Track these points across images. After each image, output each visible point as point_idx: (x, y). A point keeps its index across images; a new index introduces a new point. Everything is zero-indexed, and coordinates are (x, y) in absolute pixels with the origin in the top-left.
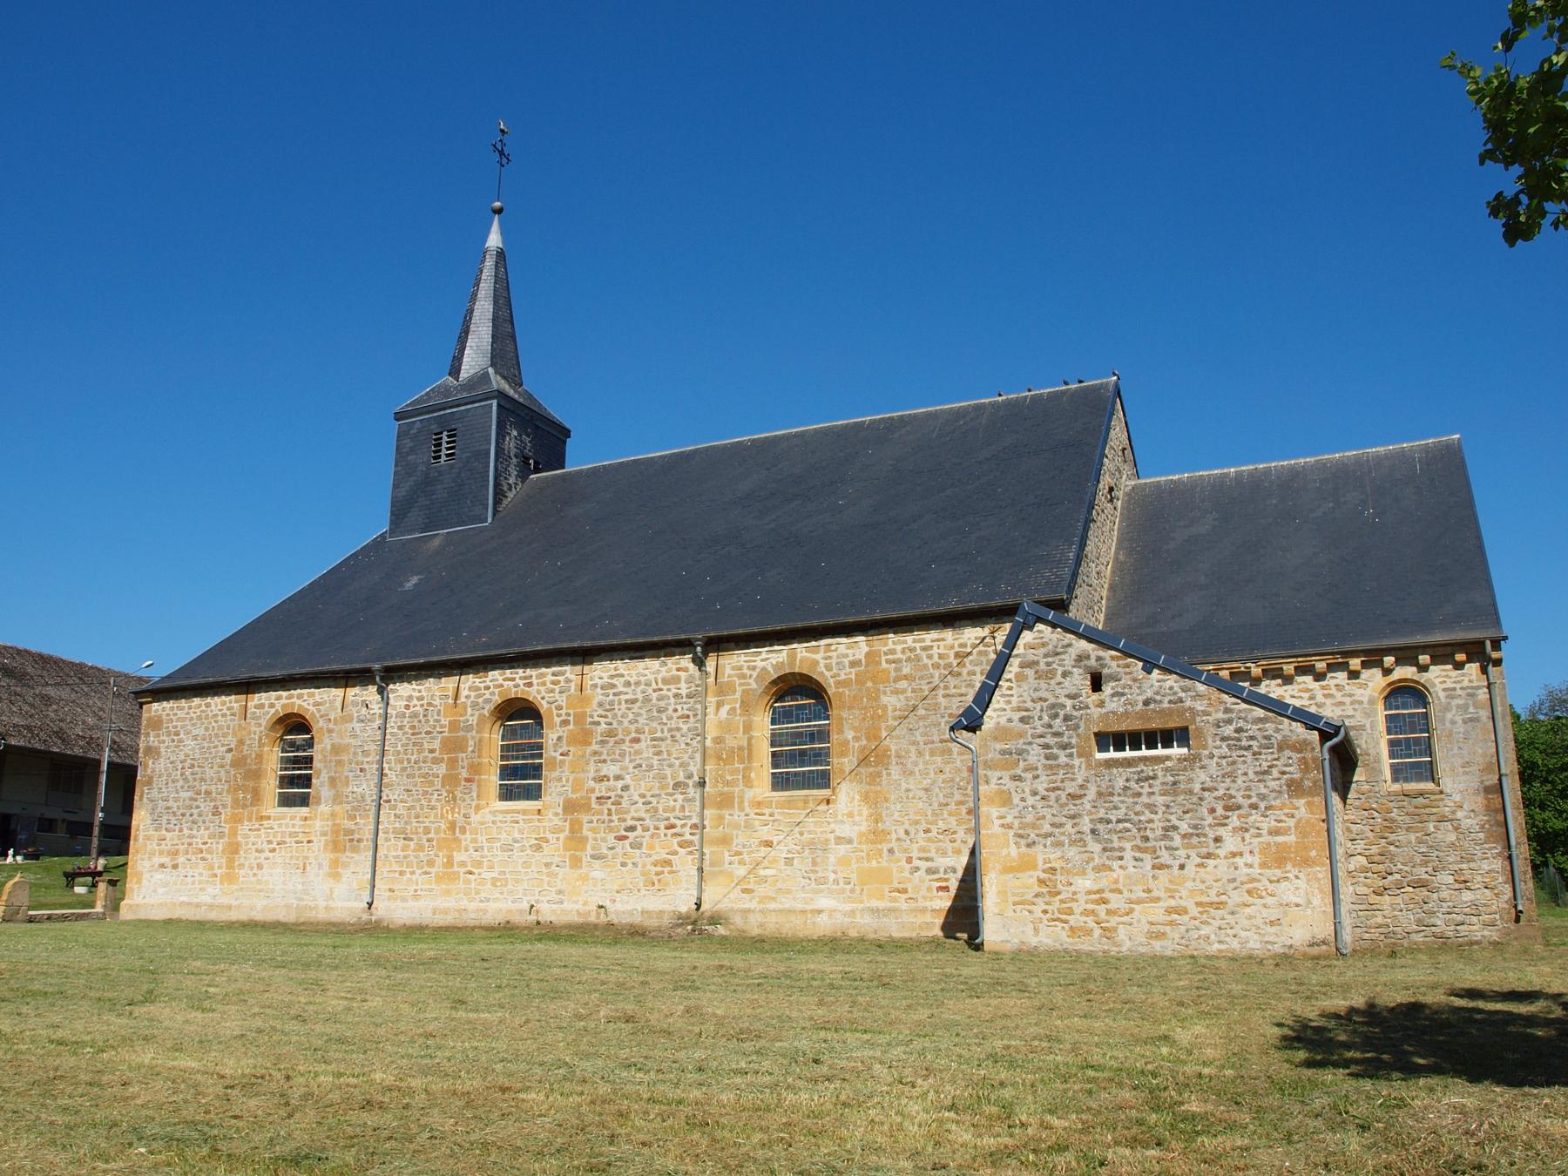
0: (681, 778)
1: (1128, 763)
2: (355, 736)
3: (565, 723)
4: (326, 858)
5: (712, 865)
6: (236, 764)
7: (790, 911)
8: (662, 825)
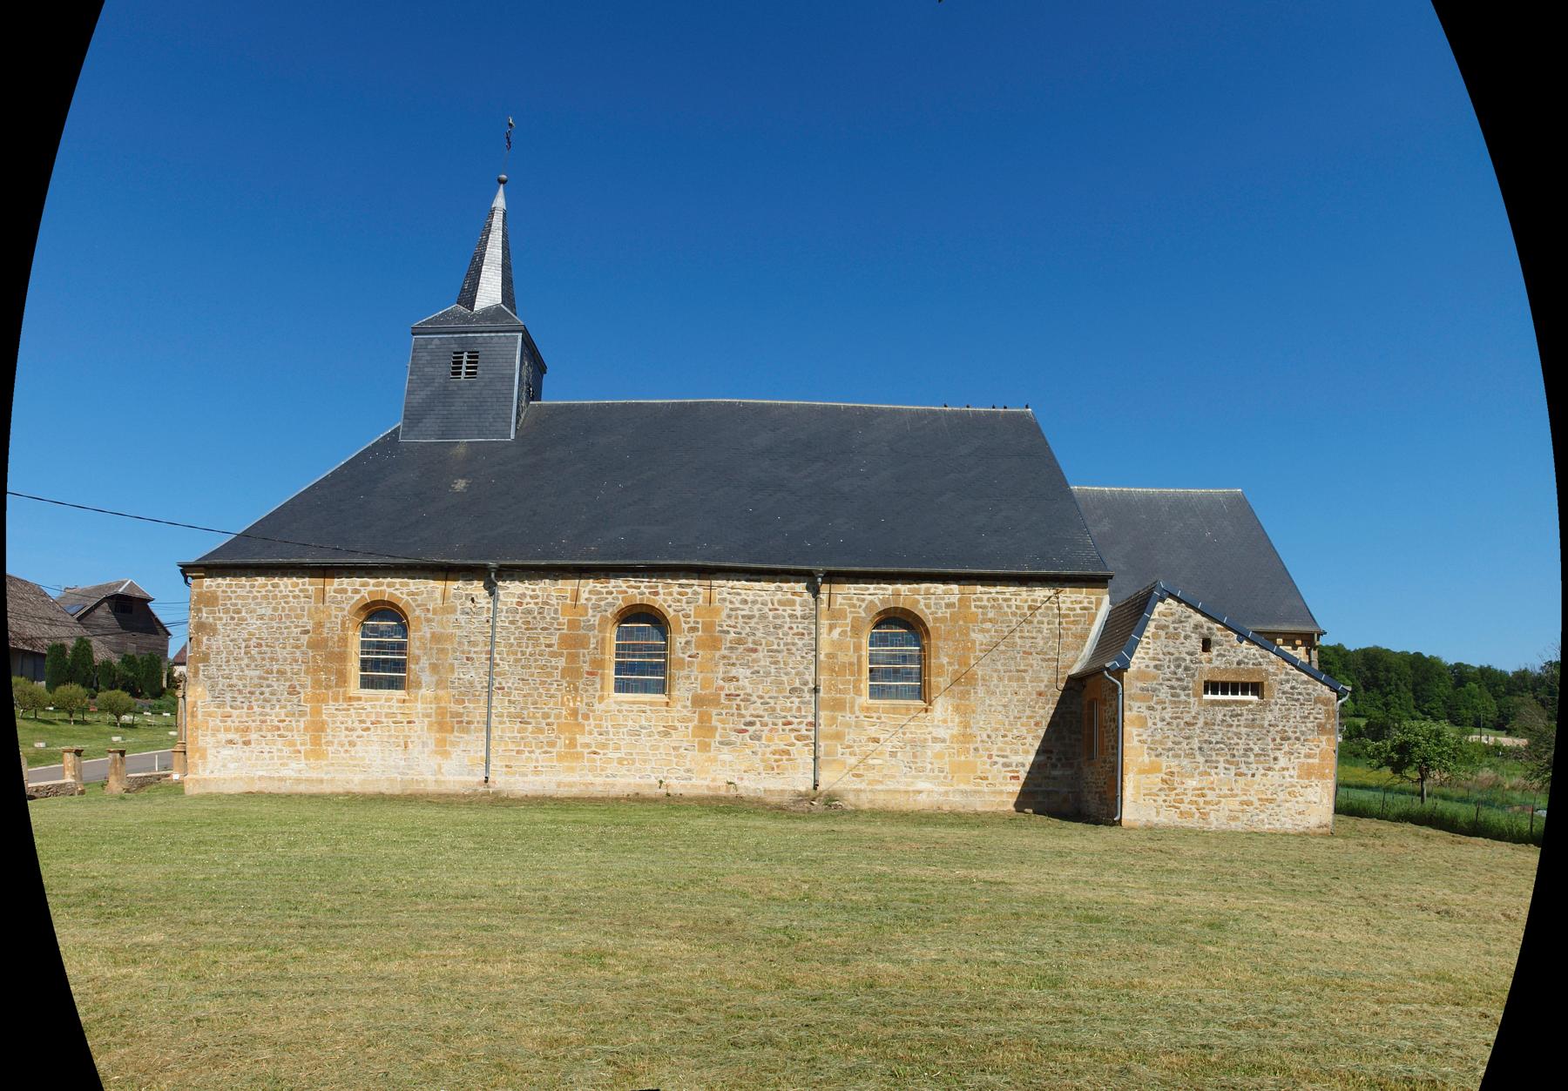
0: (797, 684)
1: (1226, 703)
2: (460, 627)
4: (432, 738)
5: (827, 754)
6: (313, 645)
7: (895, 791)
8: (780, 722)
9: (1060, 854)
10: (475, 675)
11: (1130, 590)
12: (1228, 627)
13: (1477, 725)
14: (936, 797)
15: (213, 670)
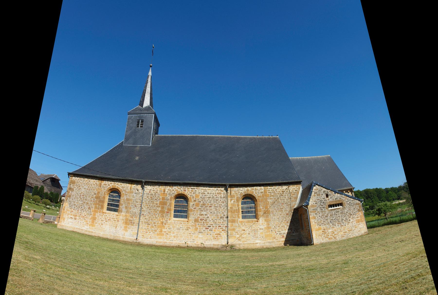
0: (222, 216)
1: (334, 209)
2: (134, 197)
3: (195, 201)
4: (123, 226)
5: (231, 234)
8: (218, 226)
9: (298, 255)
10: (136, 210)
11: (307, 184)
12: (331, 191)
13: (394, 200)
14: (262, 244)
15: (71, 200)
